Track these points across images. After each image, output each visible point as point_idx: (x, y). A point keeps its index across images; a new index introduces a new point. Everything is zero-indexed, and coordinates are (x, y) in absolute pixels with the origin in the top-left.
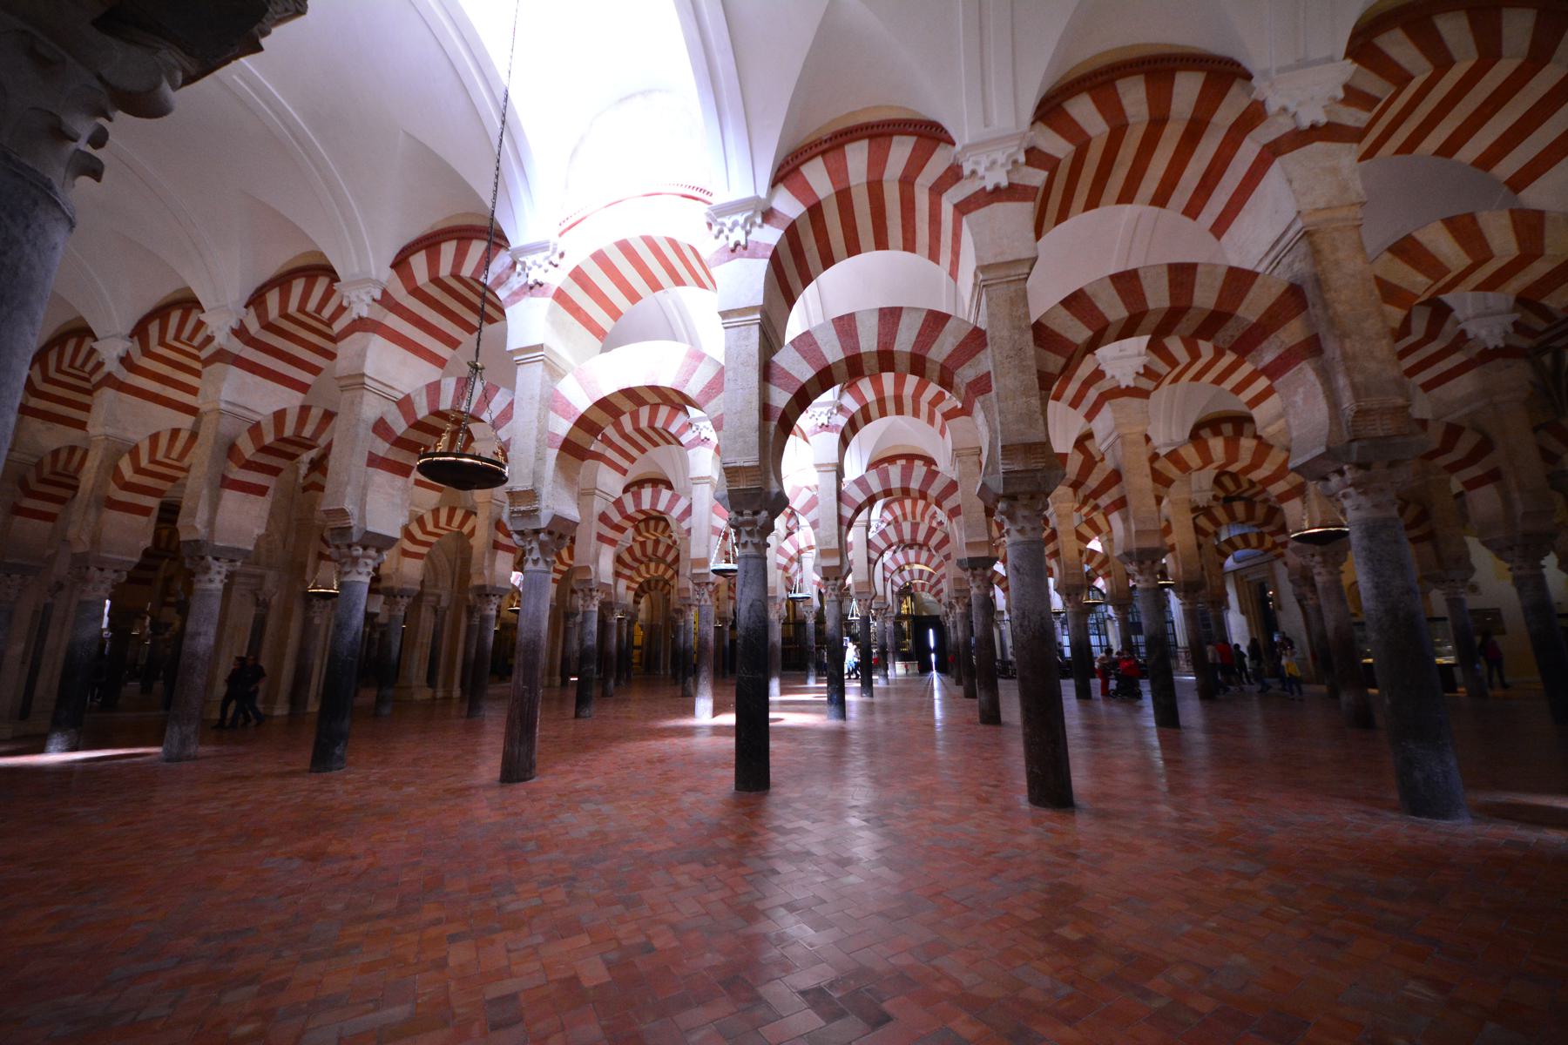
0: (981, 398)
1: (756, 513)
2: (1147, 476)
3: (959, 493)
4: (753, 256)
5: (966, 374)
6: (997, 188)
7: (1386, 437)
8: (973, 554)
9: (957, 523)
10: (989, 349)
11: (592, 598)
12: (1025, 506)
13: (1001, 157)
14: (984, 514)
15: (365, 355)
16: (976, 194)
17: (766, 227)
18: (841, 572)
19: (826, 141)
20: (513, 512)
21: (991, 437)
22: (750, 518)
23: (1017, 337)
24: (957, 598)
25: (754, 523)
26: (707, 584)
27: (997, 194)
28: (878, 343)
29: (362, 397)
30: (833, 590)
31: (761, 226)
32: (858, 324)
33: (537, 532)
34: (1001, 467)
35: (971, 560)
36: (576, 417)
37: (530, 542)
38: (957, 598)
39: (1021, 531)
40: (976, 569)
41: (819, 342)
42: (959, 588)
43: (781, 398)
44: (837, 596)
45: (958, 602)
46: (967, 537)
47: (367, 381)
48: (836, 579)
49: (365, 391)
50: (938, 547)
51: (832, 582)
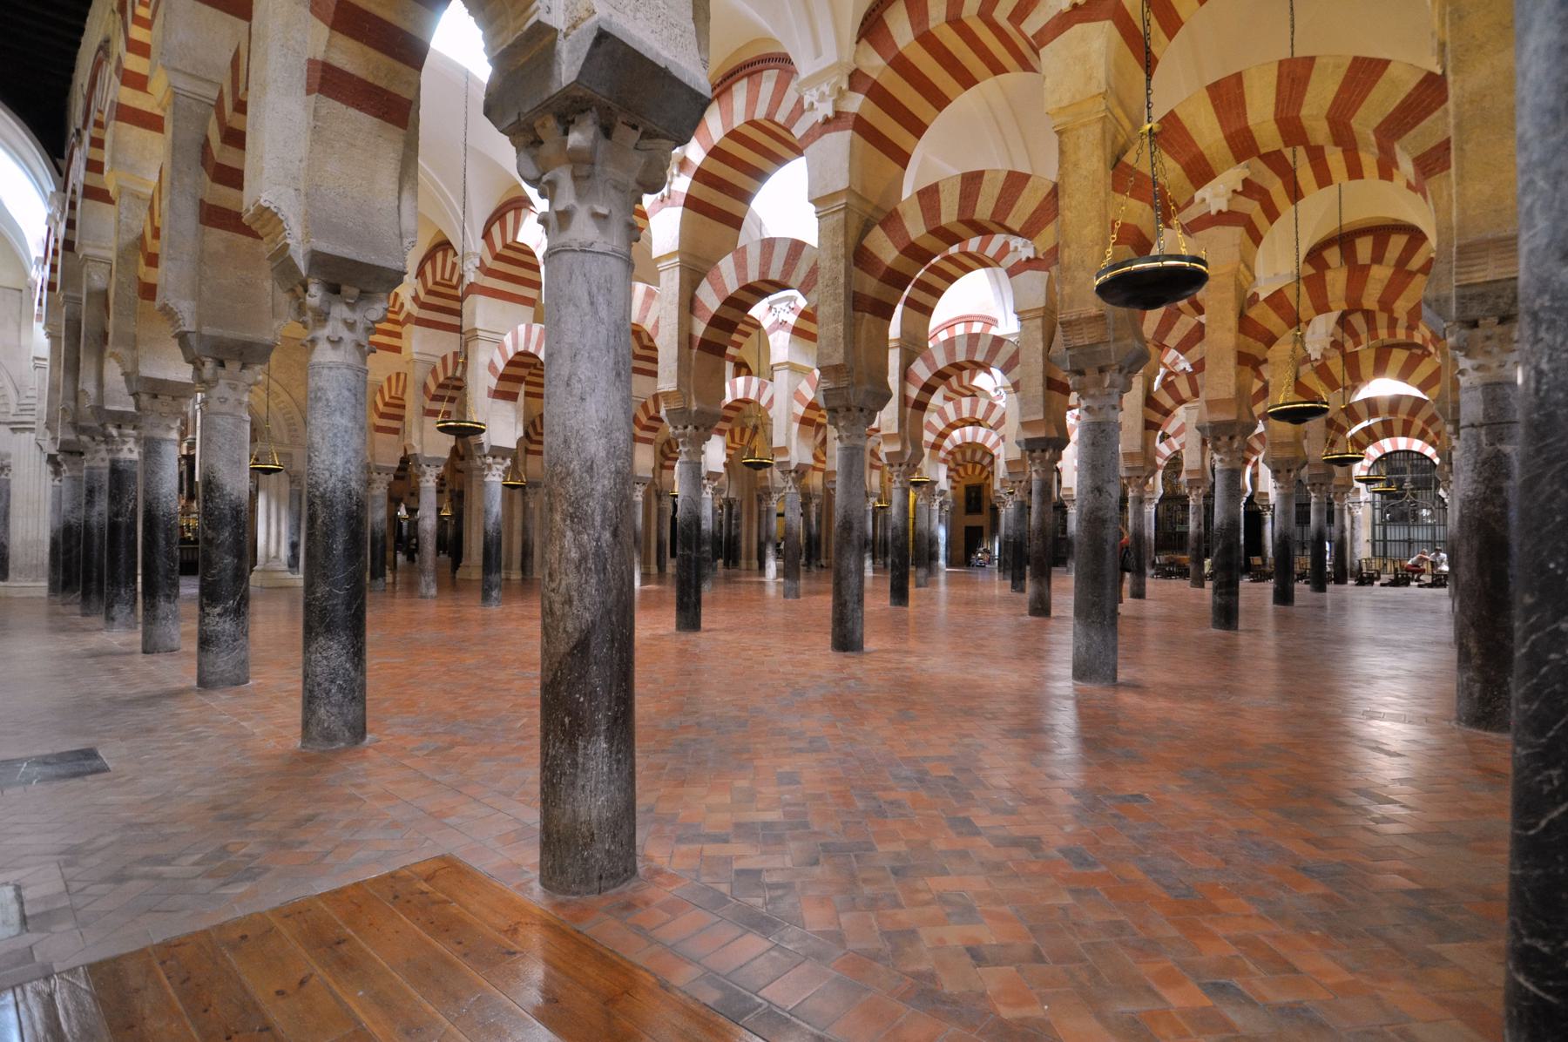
1: (686, 427)
2: (1230, 330)
4: (673, 205)
6: (827, 121)
7: (1091, 345)
8: (1030, 435)
11: (705, 486)
12: (844, 417)
13: (826, 88)
14: (1041, 389)
16: (812, 128)
17: (682, 175)
18: (903, 458)
19: (718, 85)
22: (681, 431)
25: (684, 435)
27: (829, 124)
30: (897, 476)
31: (678, 176)
32: (748, 256)
40: (1034, 451)
42: (1130, 465)
43: (700, 328)
44: (901, 482)
48: (900, 465)
51: (896, 468)
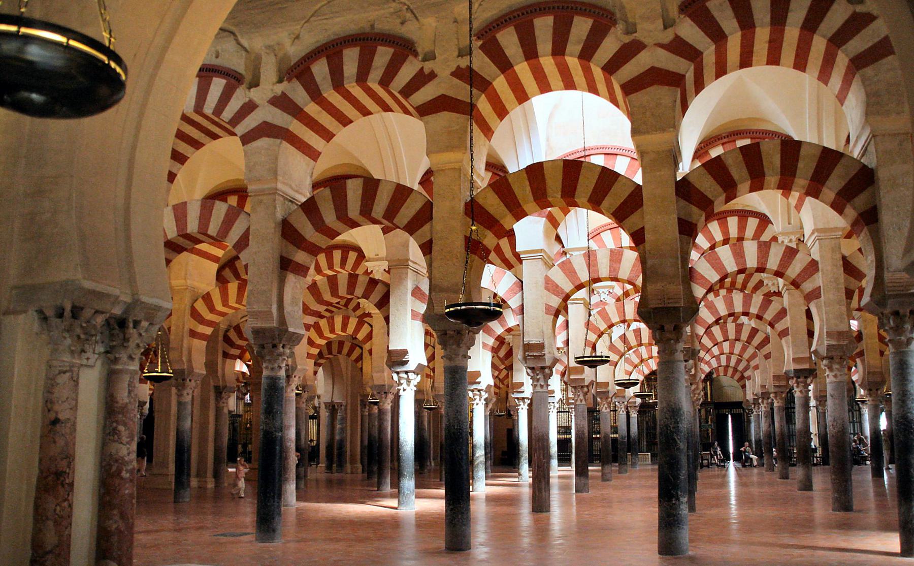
0: (815, 301)
3: (788, 317)
5: (808, 286)
9: (787, 342)
10: (820, 273)
15: (408, 246)
20: (528, 356)
21: (820, 324)
23: (835, 270)
24: (775, 393)
26: (582, 387)
28: (758, 263)
29: (407, 274)
33: (543, 368)
34: (825, 342)
35: (796, 371)
36: (564, 295)
37: (537, 375)
38: (775, 393)
39: (835, 376)
41: (722, 259)
45: (776, 397)
46: (794, 353)
47: (410, 263)
49: (409, 270)
50: (760, 346)
